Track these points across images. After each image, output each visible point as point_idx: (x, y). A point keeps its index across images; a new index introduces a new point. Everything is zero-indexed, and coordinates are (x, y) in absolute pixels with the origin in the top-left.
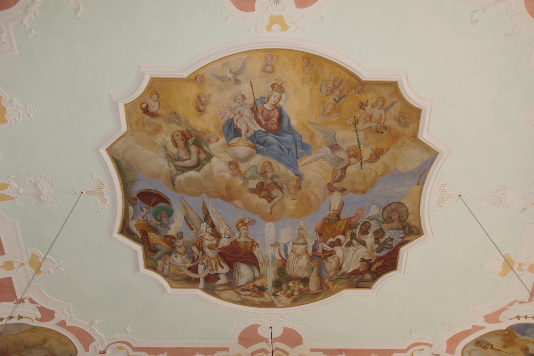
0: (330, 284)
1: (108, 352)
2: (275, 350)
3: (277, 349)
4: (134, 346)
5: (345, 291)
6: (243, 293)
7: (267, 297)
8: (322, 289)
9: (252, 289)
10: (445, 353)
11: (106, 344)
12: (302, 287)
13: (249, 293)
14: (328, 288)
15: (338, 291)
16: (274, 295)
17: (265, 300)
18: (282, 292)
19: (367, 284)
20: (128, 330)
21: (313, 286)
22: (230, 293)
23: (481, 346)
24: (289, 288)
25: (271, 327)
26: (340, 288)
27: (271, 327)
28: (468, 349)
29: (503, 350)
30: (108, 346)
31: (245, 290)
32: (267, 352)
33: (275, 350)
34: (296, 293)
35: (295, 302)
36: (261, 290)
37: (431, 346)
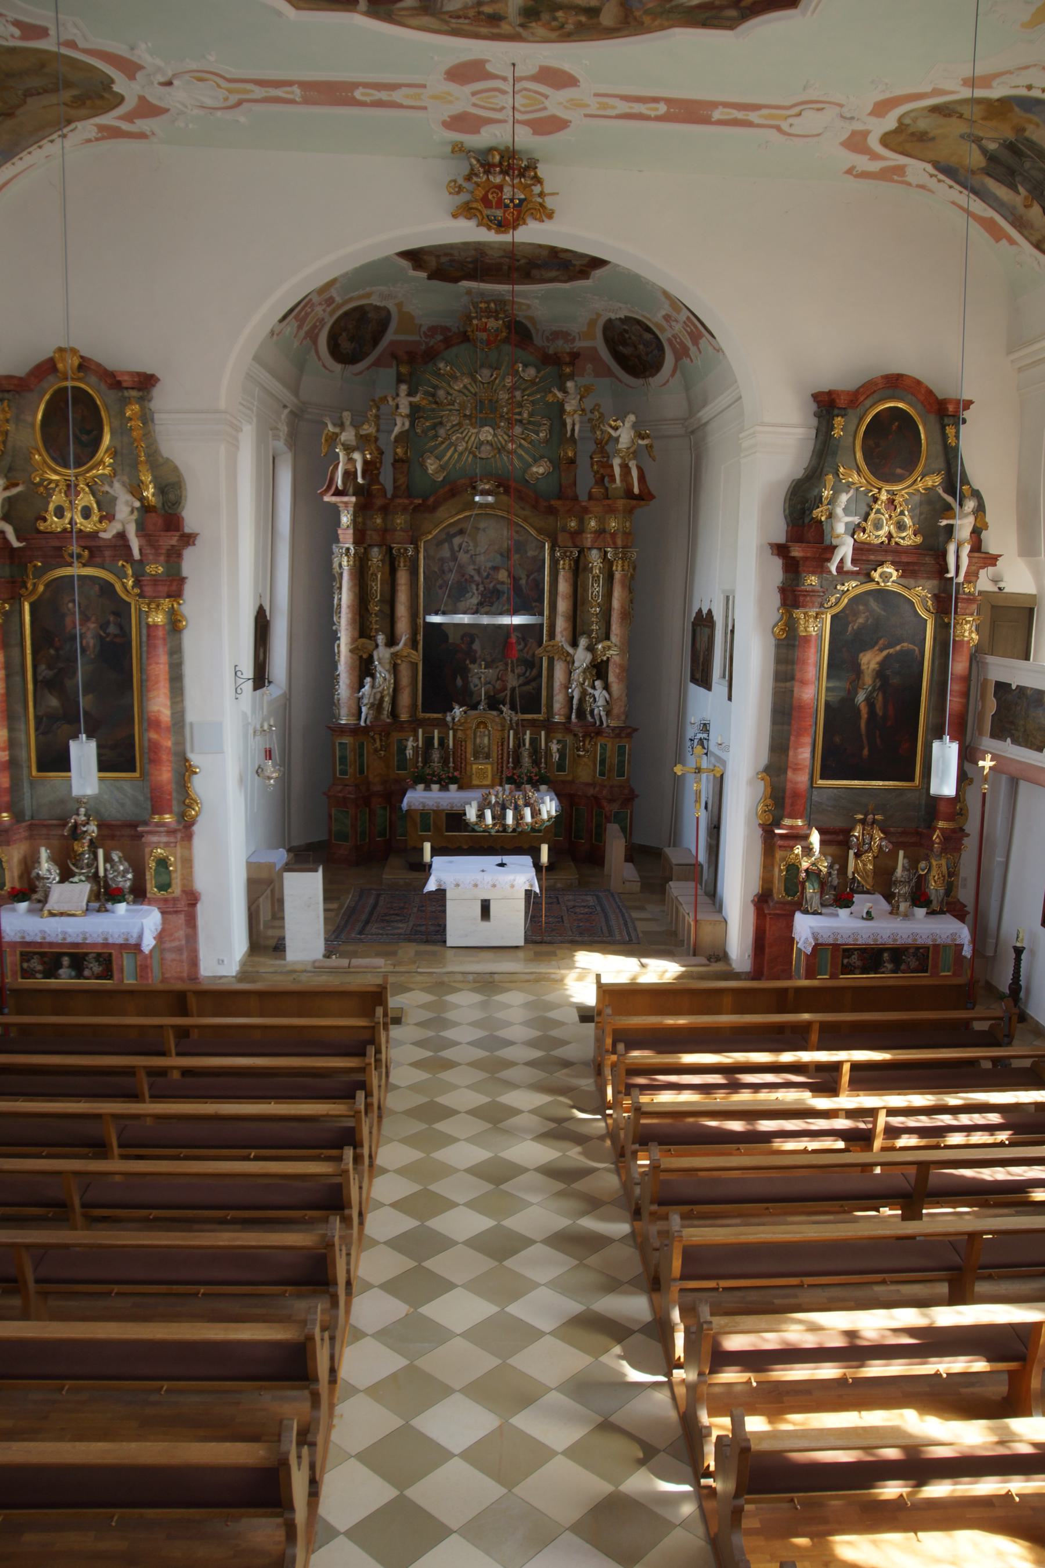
0: (647, 20)
1: (176, 82)
2: (520, 91)
3: (526, 89)
4: (228, 76)
5: (677, 30)
6: (453, 21)
7: (505, 28)
8: (628, 23)
9: (474, 16)
10: (871, 114)
11: (170, 73)
12: (583, 19)
13: (467, 21)
14: (642, 23)
15: (662, 28)
16: (522, 25)
17: (502, 32)
18: (540, 23)
19: (729, 23)
20: (212, 59)
21: (607, 18)
22: (426, 20)
23: (940, 113)
24: (555, 19)
25: (514, 65)
26: (666, 23)
27: (514, 65)
28: (913, 115)
29: (980, 122)
30: (174, 75)
31: (459, 17)
32: (503, 92)
33: (520, 91)
34: (570, 27)
35: (567, 37)
36: (495, 19)
37: (841, 106)
